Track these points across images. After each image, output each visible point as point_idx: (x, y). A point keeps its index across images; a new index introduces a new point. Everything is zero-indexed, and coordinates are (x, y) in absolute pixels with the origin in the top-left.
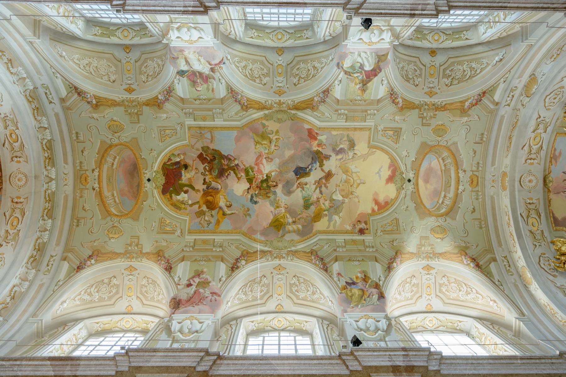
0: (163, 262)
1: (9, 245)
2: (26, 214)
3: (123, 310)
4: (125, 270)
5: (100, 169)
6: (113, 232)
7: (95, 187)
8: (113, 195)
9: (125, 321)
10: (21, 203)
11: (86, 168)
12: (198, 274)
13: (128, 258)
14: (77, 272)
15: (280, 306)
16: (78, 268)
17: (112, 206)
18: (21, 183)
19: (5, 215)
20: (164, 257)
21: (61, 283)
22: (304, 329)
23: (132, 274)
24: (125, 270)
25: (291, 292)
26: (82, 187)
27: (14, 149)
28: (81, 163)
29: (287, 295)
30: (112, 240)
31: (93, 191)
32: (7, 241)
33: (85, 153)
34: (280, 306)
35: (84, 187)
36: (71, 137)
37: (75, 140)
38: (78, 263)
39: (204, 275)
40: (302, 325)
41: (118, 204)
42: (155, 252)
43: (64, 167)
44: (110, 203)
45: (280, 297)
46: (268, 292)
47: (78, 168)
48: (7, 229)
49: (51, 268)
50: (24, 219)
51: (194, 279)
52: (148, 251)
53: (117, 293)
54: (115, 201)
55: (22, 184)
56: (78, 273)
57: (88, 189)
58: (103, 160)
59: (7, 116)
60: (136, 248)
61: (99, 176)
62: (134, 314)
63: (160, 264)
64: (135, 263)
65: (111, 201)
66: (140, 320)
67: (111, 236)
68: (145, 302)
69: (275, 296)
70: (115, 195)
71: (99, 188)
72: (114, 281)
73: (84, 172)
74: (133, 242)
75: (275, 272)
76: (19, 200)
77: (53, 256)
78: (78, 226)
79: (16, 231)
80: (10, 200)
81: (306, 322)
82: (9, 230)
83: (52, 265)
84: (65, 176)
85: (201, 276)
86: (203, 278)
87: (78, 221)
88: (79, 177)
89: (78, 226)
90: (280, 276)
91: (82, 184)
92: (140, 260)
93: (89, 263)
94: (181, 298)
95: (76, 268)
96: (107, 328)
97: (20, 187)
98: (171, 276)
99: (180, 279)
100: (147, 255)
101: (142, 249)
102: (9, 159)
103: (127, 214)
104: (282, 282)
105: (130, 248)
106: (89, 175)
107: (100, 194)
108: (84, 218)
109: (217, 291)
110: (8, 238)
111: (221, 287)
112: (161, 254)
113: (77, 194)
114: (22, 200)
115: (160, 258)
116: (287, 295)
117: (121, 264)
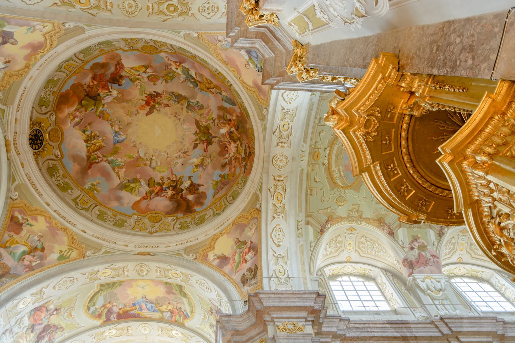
0: (385, 228)
1: (281, 217)
2: (288, 190)
3: (344, 259)
4: (347, 230)
5: (331, 148)
6: (340, 201)
7: (325, 162)
8: (339, 170)
9: (346, 268)
10: (282, 181)
11: (319, 146)
12: (415, 239)
13: (350, 221)
14: (321, 234)
15: (460, 259)
16: (321, 231)
17: (338, 179)
18: (282, 164)
19: (270, 191)
20: (386, 224)
21: (313, 244)
22: (480, 276)
23: (352, 233)
24: (347, 230)
25: (471, 249)
26: (314, 162)
27: (281, 136)
28: (316, 142)
29: (467, 251)
30: (340, 207)
31: (322, 166)
32: (278, 214)
33: (322, 134)
34: (460, 259)
35: (316, 162)
36: (315, 121)
37: (317, 123)
38: (320, 227)
39: (420, 240)
40: (479, 274)
41: (343, 177)
42: (376, 219)
43: (303, 145)
44: (337, 176)
45: (461, 252)
46: (454, 249)
47: (313, 146)
48: (274, 203)
49: (302, 231)
50: (286, 194)
51: (414, 243)
52: (369, 217)
53: (341, 247)
54: (341, 175)
55: (283, 165)
56: (323, 236)
57: (319, 164)
58: (336, 141)
59: (289, 111)
60: (357, 214)
61: (329, 153)
62: (353, 262)
63: (383, 229)
64: (355, 225)
65: (337, 175)
66: (359, 267)
67: (339, 204)
68: (362, 254)
69: (458, 251)
70: (341, 170)
71: (328, 163)
72: (339, 239)
73: (318, 150)
74: (353, 209)
75: (461, 234)
76: (280, 179)
77: (299, 221)
78: (311, 195)
79: (281, 205)
80: (272, 178)
81: (483, 272)
82: (276, 204)
83: (302, 229)
84: (302, 153)
85: (419, 241)
86: (420, 242)
87: (311, 190)
88: (312, 154)
89: (311, 195)
90: (463, 237)
91: (314, 160)
92: (359, 223)
93: (327, 226)
94: (411, 259)
95: (319, 231)
96: (334, 273)
97: (281, 167)
98: (395, 240)
99: (403, 243)
100: (368, 220)
101: (362, 214)
102: (275, 144)
103: (350, 186)
104: (464, 242)
105: (351, 213)
106: (321, 153)
107: (329, 169)
108: (316, 188)
109: (435, 254)
110: (278, 211)
111: (436, 251)
112: (382, 221)
113: (309, 168)
114: (282, 178)
115: (382, 224)
116: (467, 251)
117: (344, 225)
